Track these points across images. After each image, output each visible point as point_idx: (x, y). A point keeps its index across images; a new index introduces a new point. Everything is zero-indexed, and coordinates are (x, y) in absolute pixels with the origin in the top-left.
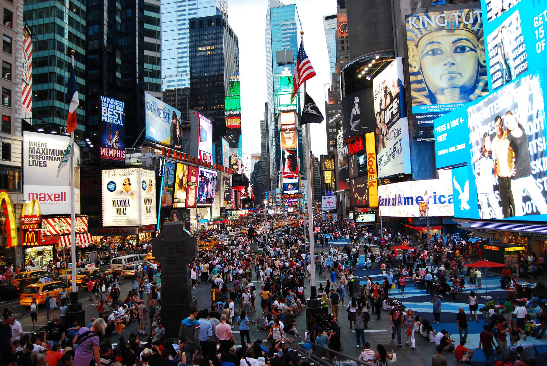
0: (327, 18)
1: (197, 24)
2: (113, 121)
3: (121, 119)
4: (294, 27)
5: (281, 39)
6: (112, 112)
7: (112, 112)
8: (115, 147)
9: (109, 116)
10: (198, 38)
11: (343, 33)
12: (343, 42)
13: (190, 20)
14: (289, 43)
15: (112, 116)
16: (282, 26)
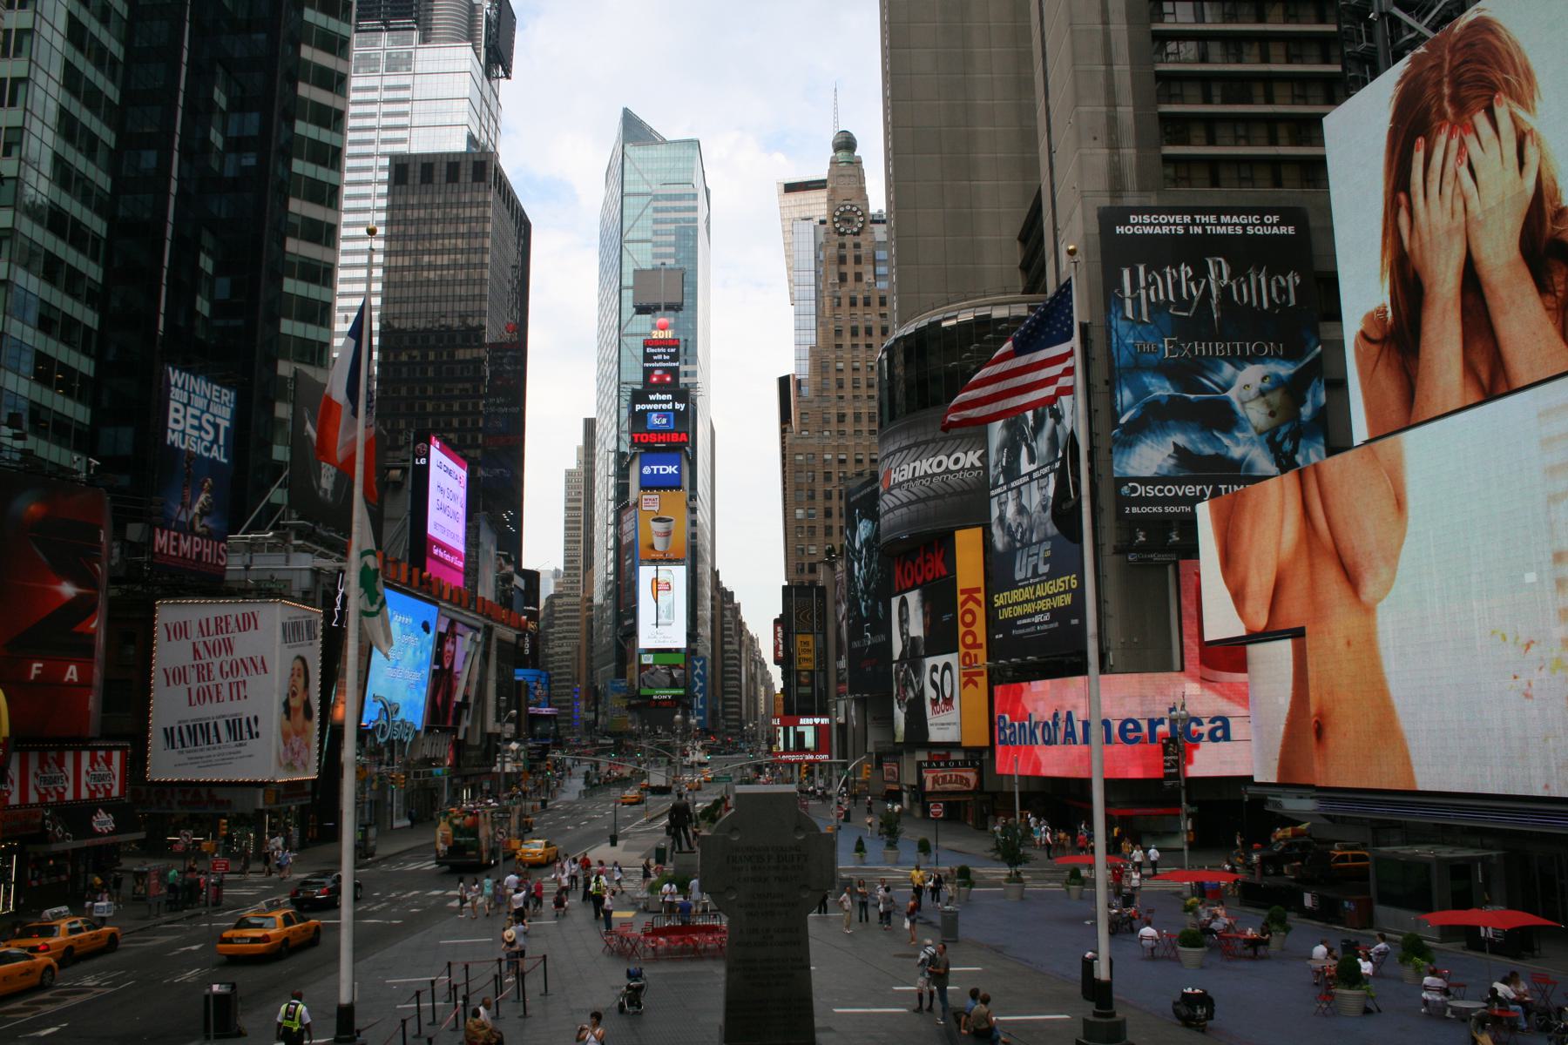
0: (790, 188)
1: (414, 175)
2: (198, 449)
3: (221, 442)
4: (691, 203)
5: (649, 235)
6: (199, 418)
7: (199, 418)
8: (198, 528)
9: (189, 431)
10: (413, 214)
11: (844, 234)
12: (842, 260)
13: (394, 158)
14: (672, 250)
15: (196, 433)
16: (656, 198)
